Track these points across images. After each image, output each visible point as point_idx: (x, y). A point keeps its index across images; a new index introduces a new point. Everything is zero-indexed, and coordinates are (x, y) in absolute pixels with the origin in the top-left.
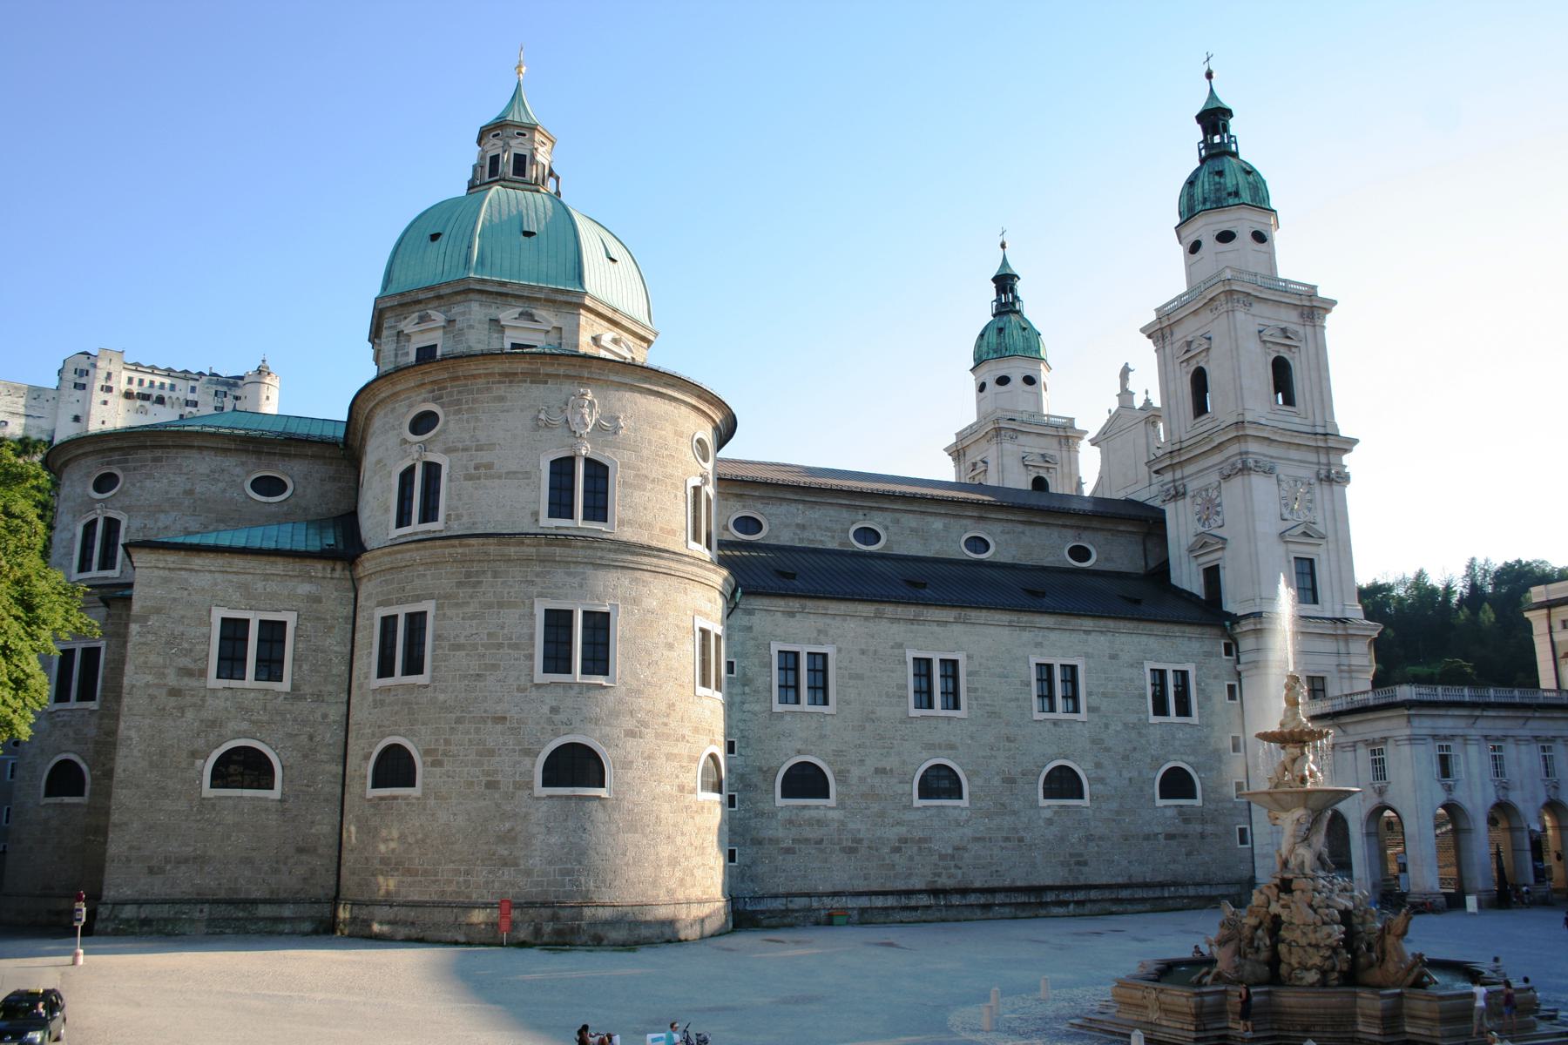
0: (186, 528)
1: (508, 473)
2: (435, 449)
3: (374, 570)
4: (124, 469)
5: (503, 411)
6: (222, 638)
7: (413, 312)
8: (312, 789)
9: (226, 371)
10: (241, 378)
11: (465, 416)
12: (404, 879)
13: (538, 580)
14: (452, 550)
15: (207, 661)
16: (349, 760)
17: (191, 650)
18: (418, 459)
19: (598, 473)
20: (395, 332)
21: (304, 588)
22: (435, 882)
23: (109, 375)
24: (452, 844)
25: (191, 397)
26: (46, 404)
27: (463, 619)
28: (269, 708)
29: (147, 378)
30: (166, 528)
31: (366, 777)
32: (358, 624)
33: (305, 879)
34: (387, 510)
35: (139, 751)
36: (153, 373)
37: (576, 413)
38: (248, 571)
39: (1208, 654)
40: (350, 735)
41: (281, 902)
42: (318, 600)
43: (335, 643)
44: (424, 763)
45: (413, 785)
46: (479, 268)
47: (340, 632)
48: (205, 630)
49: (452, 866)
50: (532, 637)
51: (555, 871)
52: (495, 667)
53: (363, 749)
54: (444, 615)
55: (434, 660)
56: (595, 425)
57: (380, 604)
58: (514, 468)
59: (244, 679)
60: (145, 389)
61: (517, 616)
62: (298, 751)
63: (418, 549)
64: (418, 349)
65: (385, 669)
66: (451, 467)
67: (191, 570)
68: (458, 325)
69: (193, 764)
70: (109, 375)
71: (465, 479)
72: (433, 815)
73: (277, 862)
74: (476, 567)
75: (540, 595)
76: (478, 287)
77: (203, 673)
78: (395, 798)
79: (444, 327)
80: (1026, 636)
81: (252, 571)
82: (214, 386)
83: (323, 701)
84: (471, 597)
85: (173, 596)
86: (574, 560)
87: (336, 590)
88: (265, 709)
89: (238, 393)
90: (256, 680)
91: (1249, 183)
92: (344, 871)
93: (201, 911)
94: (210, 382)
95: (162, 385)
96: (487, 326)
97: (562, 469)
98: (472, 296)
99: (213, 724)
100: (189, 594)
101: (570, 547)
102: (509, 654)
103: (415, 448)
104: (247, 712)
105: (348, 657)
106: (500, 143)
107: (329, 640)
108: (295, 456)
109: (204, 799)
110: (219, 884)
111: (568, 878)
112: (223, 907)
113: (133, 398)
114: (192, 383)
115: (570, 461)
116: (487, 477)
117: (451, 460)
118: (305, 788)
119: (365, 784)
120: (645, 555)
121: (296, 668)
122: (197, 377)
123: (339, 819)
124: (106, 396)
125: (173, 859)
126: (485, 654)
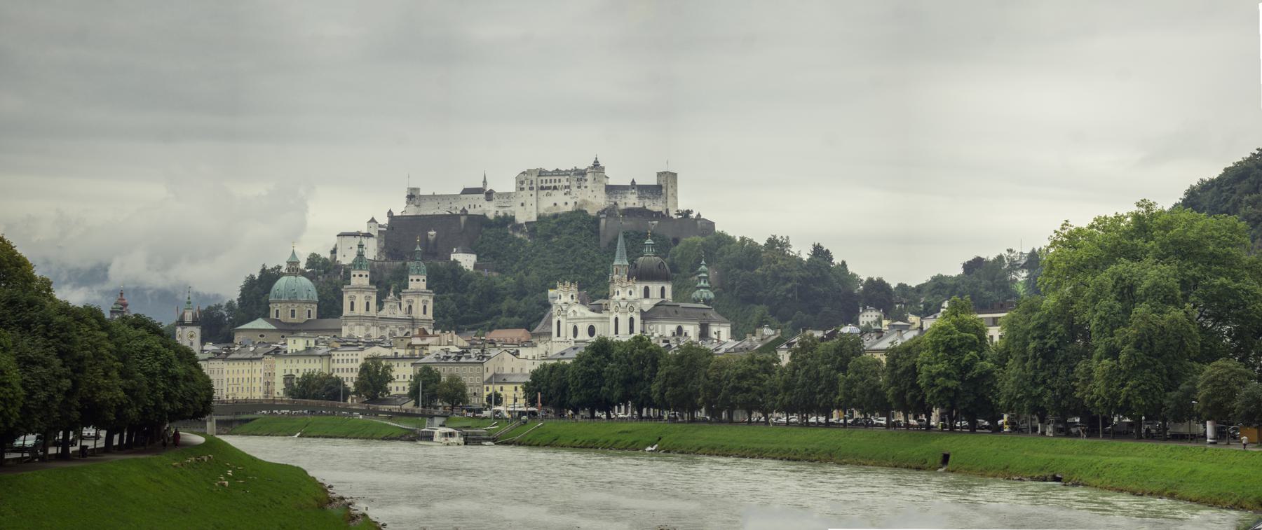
9: (582, 167)
23: (532, 182)
25: (567, 184)
29: (548, 178)
60: (548, 185)
70: (532, 182)
94: (575, 174)
114: (567, 177)
124: (532, 192)
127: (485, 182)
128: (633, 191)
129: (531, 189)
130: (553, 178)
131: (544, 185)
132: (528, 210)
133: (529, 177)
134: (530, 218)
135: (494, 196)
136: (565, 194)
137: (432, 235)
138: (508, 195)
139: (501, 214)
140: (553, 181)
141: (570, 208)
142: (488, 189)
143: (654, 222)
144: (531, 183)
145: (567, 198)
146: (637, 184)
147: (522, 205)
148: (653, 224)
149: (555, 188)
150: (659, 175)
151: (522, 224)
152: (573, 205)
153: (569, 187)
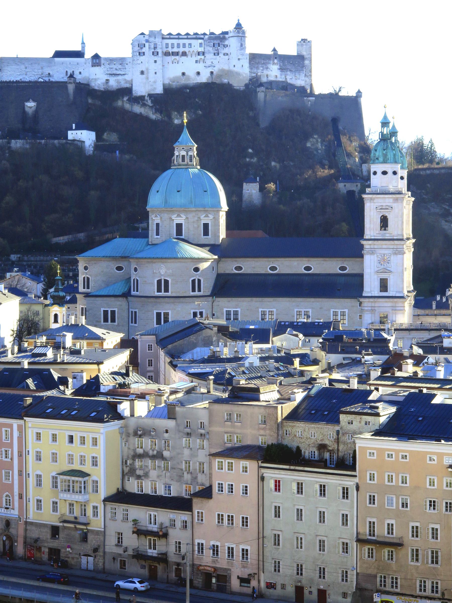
10: (227, 33)
19: (166, 282)
21: (119, 303)
25: (201, 50)
26: (127, 66)
29: (175, 42)
36: (179, 38)
39: (353, 306)
42: (121, 305)
60: (175, 50)
70: (155, 44)
75: (155, 309)
77: (100, 322)
80: (294, 304)
89: (226, 43)
91: (383, 154)
94: (210, 38)
97: (159, 282)
113: (170, 55)
114: (200, 41)
122: (202, 36)
124: (156, 58)
127: (83, 43)
128: (276, 61)
129: (155, 54)
130: (181, 42)
131: (170, 50)
132: (152, 79)
133: (152, 39)
134: (155, 88)
135: (102, 62)
136: (196, 62)
137: (31, 107)
138: (122, 61)
139: (114, 84)
141: (204, 78)
143: (311, 98)
144: (155, 48)
145: (200, 67)
147: (142, 73)
148: (309, 101)
149: (184, 54)
151: (144, 97)
152: (209, 75)
153: (203, 54)
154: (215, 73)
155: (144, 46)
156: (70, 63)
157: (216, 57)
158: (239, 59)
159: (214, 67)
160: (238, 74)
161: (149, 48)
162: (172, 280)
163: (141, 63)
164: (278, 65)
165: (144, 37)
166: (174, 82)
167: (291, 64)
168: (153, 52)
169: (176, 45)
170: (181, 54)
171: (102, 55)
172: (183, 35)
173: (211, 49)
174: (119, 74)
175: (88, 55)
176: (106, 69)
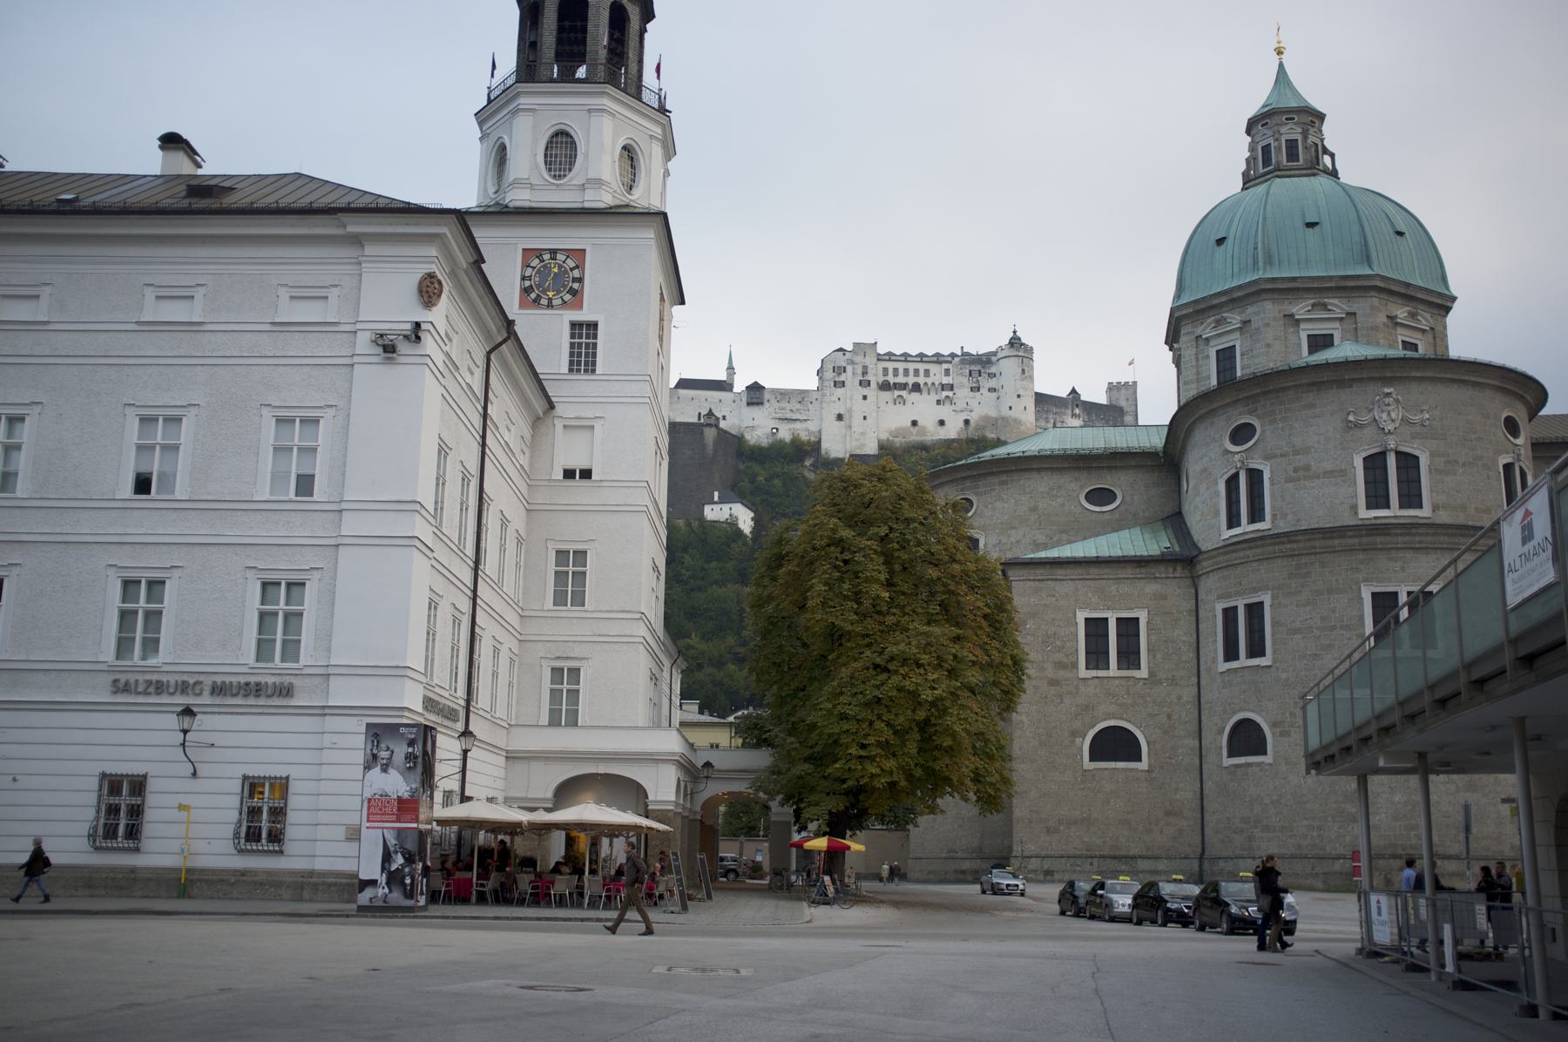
0: (1035, 541)
1: (1325, 473)
2: (1256, 456)
3: (1212, 568)
4: (976, 494)
5: (1313, 417)
6: (1087, 635)
7: (1209, 317)
8: (1174, 761)
9: (979, 345)
10: (995, 354)
11: (1280, 425)
12: (1264, 835)
13: (1362, 567)
14: (1282, 547)
15: (1077, 655)
16: (1203, 735)
17: (1063, 647)
18: (1241, 468)
19: (1408, 463)
20: (1193, 337)
21: (1151, 588)
22: (1291, 837)
23: (865, 367)
24: (1305, 803)
25: (946, 380)
27: (1297, 606)
28: (1131, 692)
29: (901, 366)
30: (1018, 542)
31: (1221, 748)
32: (1200, 616)
33: (1174, 838)
34: (1217, 514)
35: (1031, 732)
36: (906, 361)
37: (1383, 411)
38: (1102, 577)
40: (1202, 713)
41: (1156, 858)
42: (1165, 597)
43: (1182, 634)
44: (1273, 734)
45: (1265, 753)
46: (1268, 267)
47: (1186, 623)
48: (1072, 629)
49: (1305, 822)
50: (1362, 617)
51: (1400, 826)
52: (1330, 646)
53: (1216, 724)
54: (1280, 604)
55: (1273, 645)
56: (1402, 419)
57: (1220, 597)
58: (1329, 466)
59: (1108, 669)
60: (901, 379)
61: (1346, 601)
62: (1160, 728)
63: (1251, 548)
64: (1217, 351)
65: (1231, 654)
66: (1272, 472)
67: (1056, 580)
68: (1254, 325)
69: (1073, 742)
70: (865, 367)
71: (1286, 482)
72: (1285, 778)
73: (1150, 824)
74: (1304, 560)
75: (1366, 580)
76: (1269, 286)
77: (1075, 665)
78: (1249, 765)
79: (1240, 328)
81: (1106, 576)
82: (967, 366)
83: (1177, 684)
84: (1303, 586)
85: (1043, 602)
86: (1394, 546)
87: (1179, 588)
88: (1128, 693)
89: (993, 370)
90: (1118, 669)
92: (1207, 831)
93: (1091, 864)
94: (963, 362)
95: (916, 372)
96: (1281, 322)
97: (1375, 464)
98: (1264, 296)
99: (1087, 708)
100: (1057, 600)
101: (1389, 534)
102: (1342, 634)
103: (1237, 457)
104: (1113, 697)
105: (1195, 644)
106: (1269, 133)
107: (1177, 631)
108: (1122, 468)
109: (1085, 771)
110: (1104, 842)
111: (1413, 833)
112: (1108, 861)
114: (945, 366)
115: (1382, 455)
116: (1305, 478)
117: (1271, 466)
118: (1169, 760)
119: (1221, 754)
120: (1462, 535)
121: (1151, 657)
122: (950, 359)
123: (1199, 786)
124: (865, 391)
125: (1065, 821)
126: (1319, 637)
127: (731, 368)
128: (1077, 411)
129: (865, 383)
130: (911, 367)
131: (891, 379)
133: (858, 359)
134: (863, 445)
135: (767, 396)
136: (938, 402)
138: (802, 395)
139: (785, 434)
140: (911, 373)
141: (953, 430)
142: (740, 386)
144: (865, 373)
145: (945, 412)
146: (1082, 398)
147: (840, 417)
149: (916, 388)
150: (1112, 388)
152: (961, 425)
153: (951, 387)
154: (972, 423)
155: (845, 372)
156: (706, 400)
157: (974, 394)
158: (1019, 396)
159: (971, 411)
160: (1018, 422)
161: (853, 373)
162: (1433, 455)
163: (837, 399)
164: (1081, 419)
165: (844, 354)
166: (896, 437)
167: (1102, 419)
168: (861, 381)
169: (901, 371)
170: (911, 387)
171: (767, 384)
172: (914, 354)
173: (965, 380)
174: (795, 420)
175: (740, 386)
176: (772, 410)
